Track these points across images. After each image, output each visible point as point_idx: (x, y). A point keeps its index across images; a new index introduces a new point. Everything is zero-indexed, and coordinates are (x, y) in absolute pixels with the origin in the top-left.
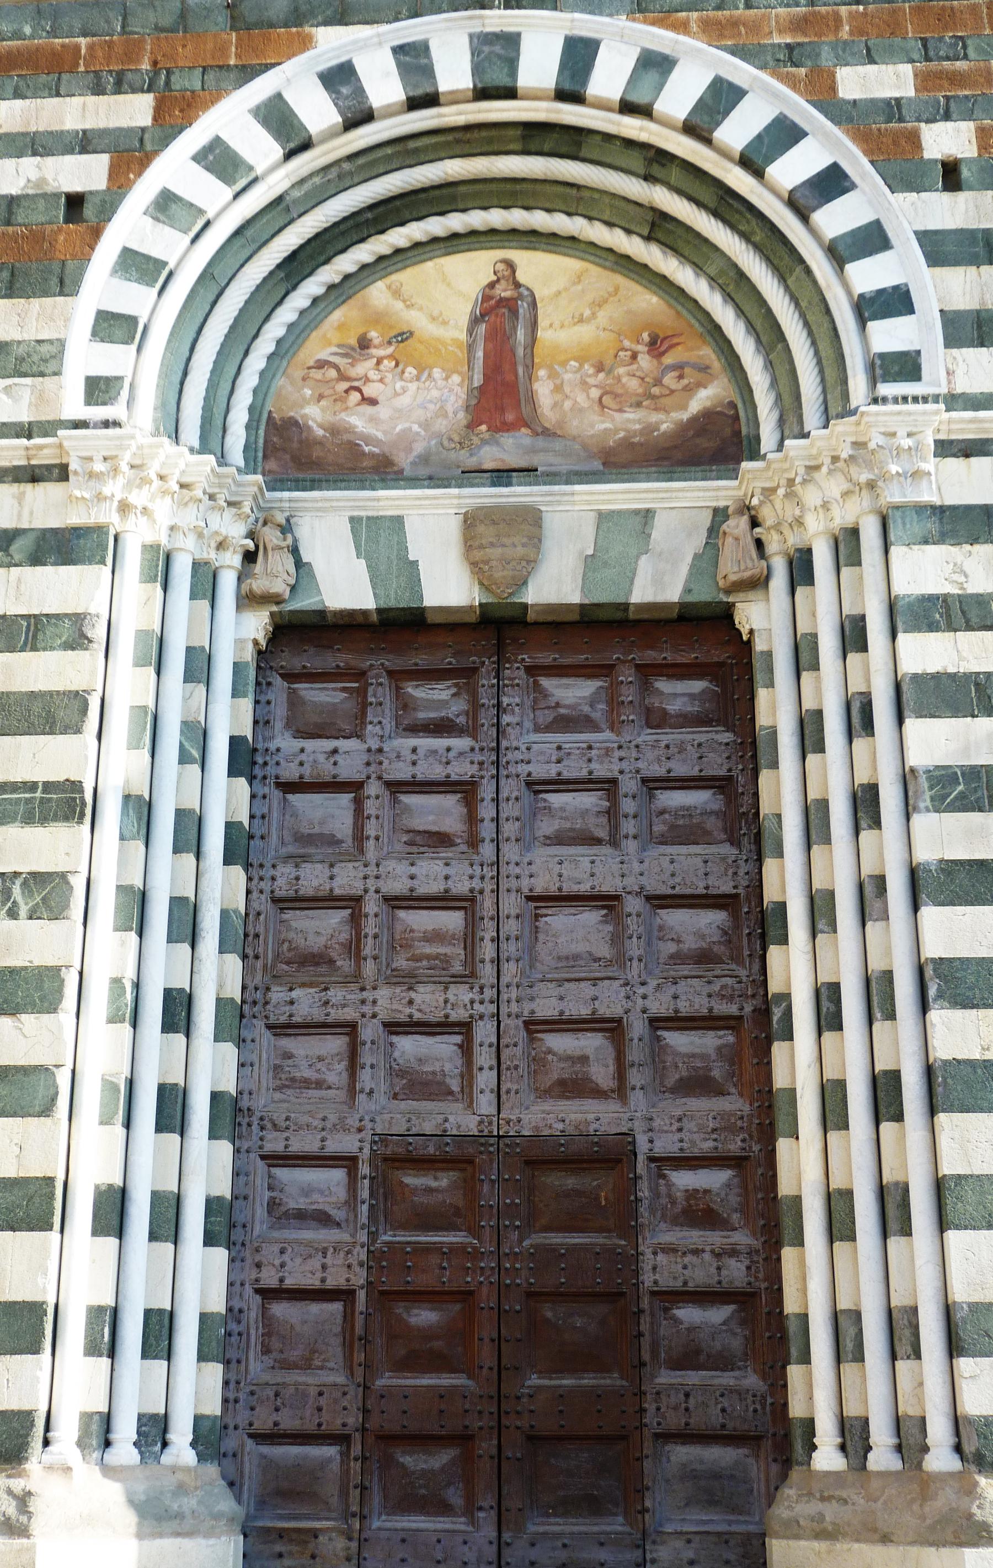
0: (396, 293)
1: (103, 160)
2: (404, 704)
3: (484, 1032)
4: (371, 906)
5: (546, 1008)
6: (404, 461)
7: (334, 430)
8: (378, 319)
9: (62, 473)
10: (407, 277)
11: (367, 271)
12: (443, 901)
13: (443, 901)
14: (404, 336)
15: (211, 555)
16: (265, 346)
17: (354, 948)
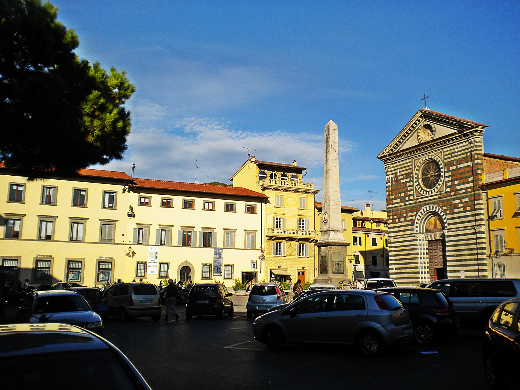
0: (431, 220)
1: (414, 217)
2: (434, 245)
3: (438, 262)
4: (433, 256)
5: (440, 261)
6: (432, 231)
7: (429, 229)
8: (430, 222)
9: (414, 236)
10: (431, 219)
11: (429, 219)
12: (436, 256)
13: (436, 256)
14: (431, 223)
15: (424, 238)
16: (425, 224)
17: (433, 258)
